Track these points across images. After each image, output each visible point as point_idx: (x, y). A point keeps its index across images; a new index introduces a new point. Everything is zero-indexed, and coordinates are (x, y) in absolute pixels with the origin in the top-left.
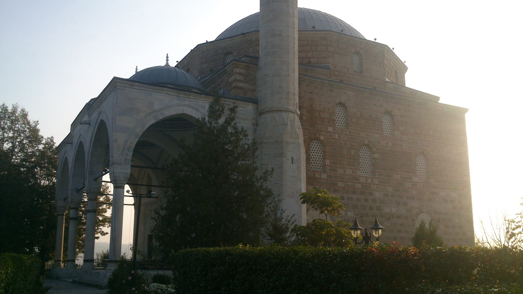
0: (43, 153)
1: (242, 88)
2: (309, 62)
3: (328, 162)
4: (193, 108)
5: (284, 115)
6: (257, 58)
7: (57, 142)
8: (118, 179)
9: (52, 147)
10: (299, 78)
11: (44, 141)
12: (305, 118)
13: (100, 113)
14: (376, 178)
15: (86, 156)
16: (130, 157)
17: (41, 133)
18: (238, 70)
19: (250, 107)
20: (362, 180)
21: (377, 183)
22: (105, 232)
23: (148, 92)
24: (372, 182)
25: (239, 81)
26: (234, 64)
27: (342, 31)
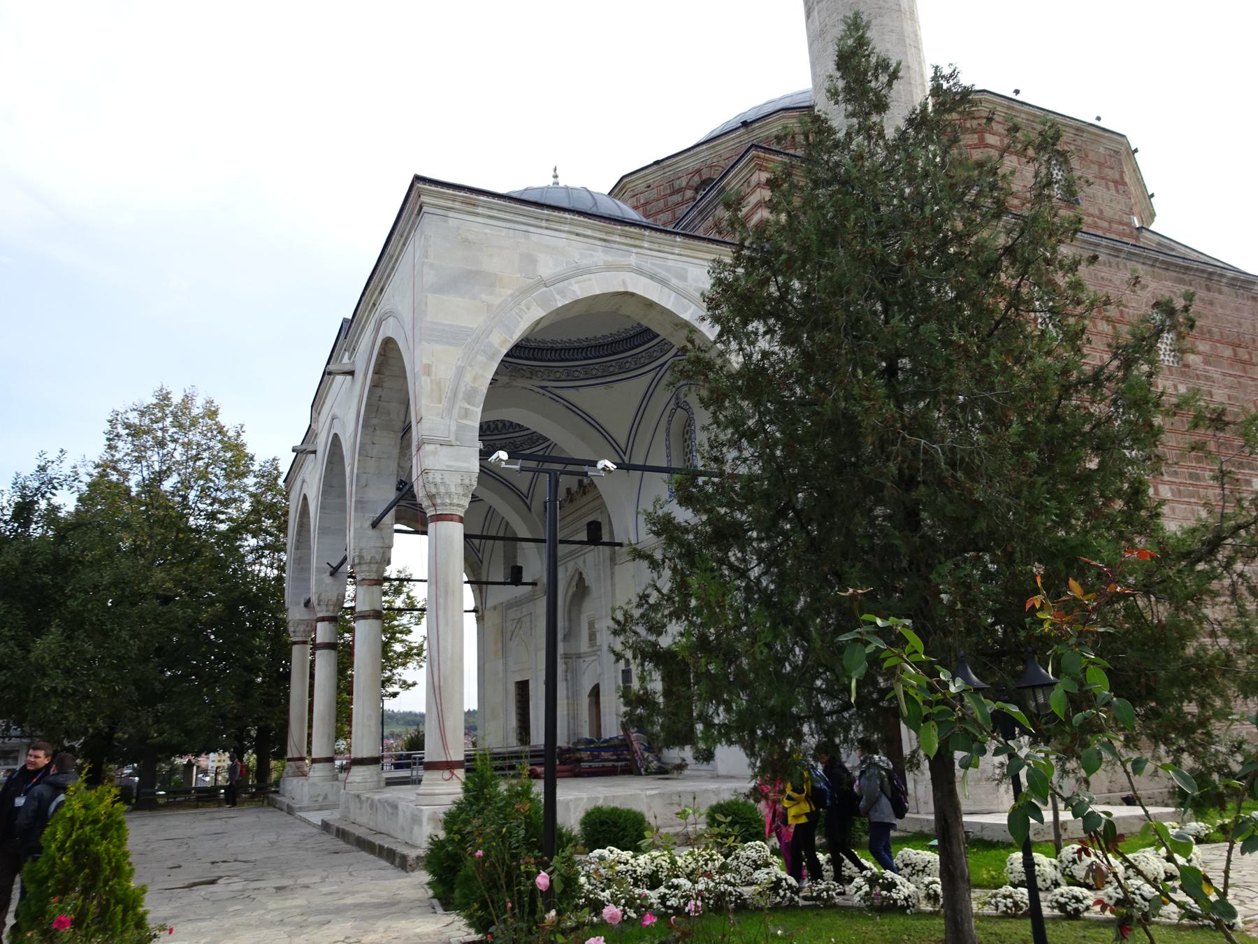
4: (652, 277)
7: (284, 468)
8: (442, 490)
11: (256, 468)
14: (1164, 483)
15: (347, 461)
17: (249, 450)
22: (410, 682)
23: (517, 226)
26: (752, 159)
27: (1017, 92)
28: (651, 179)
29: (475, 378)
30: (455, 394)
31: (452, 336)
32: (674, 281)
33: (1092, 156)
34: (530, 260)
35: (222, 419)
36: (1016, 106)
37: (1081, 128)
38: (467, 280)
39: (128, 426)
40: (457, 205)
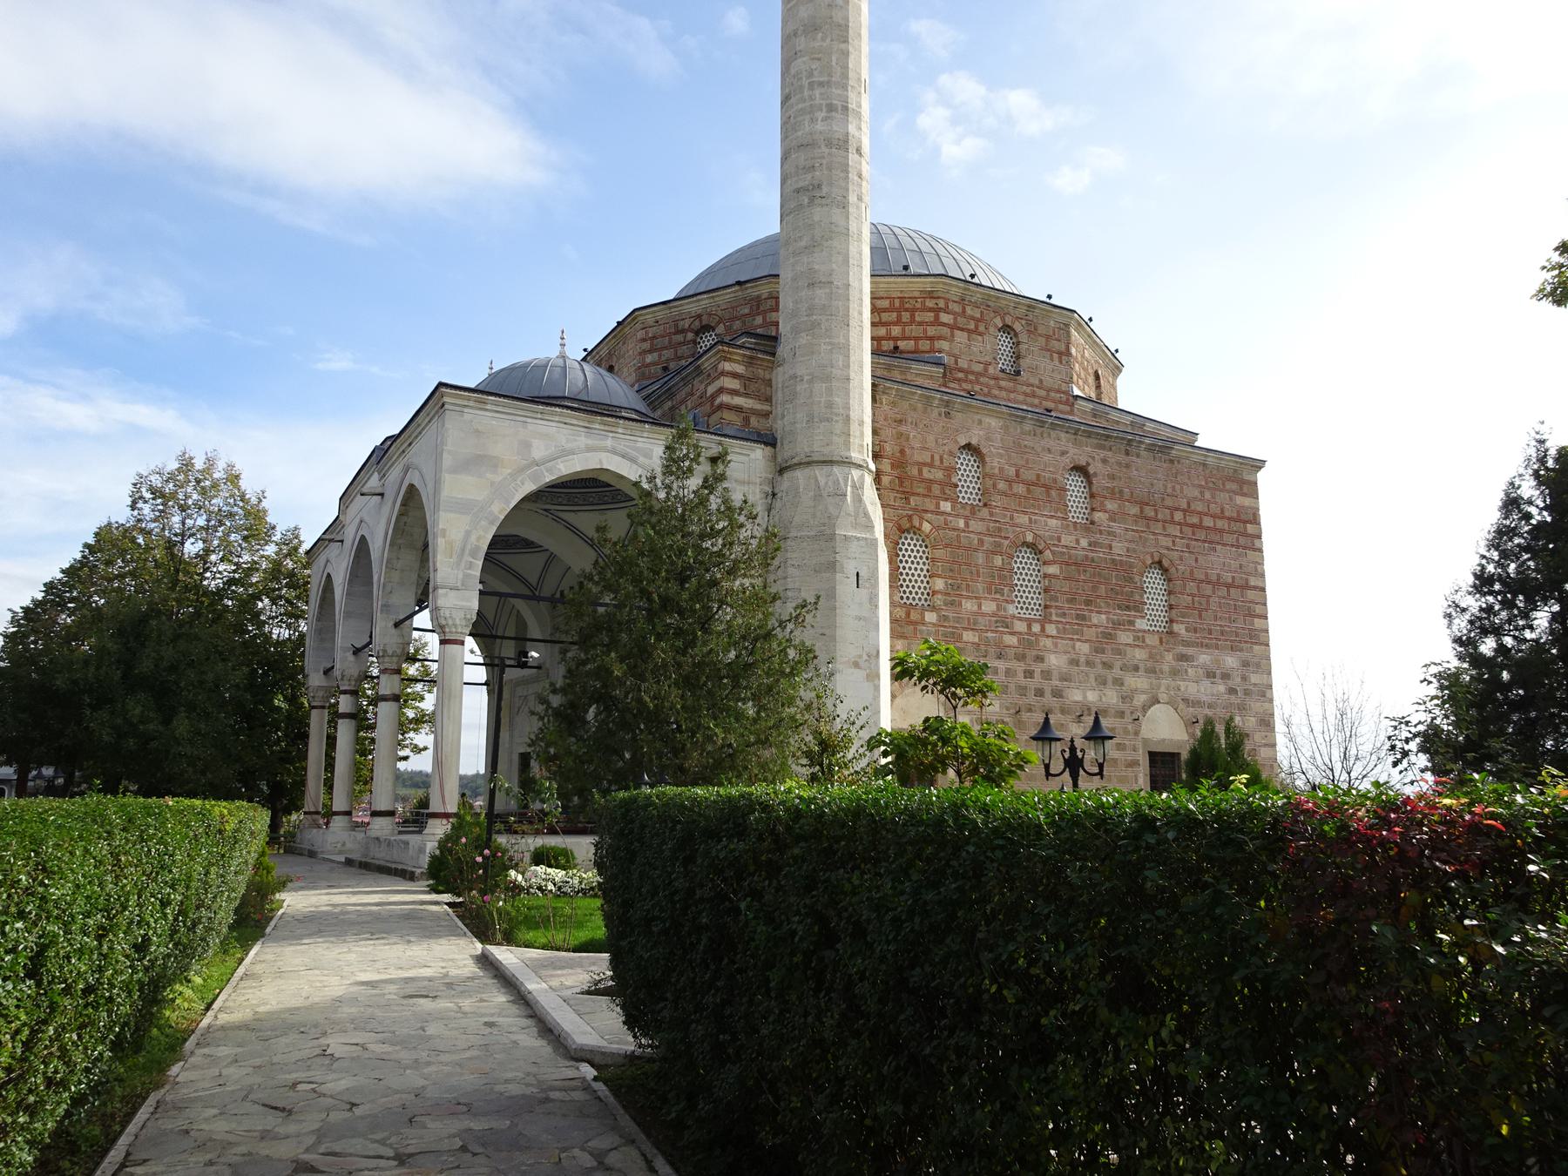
0: (277, 566)
1: (738, 409)
2: (896, 348)
3: (939, 584)
5: (836, 469)
6: (775, 339)
7: (308, 540)
9: (296, 549)
10: (873, 385)
12: (885, 480)
13: (406, 470)
14: (1051, 622)
16: (477, 572)
17: (270, 519)
18: (728, 366)
19: (759, 453)
20: (1020, 627)
21: (1054, 633)
24: (1043, 629)
25: (734, 392)
28: (660, 315)
29: (478, 539)
30: (463, 550)
31: (463, 507)
32: (641, 459)
33: (1041, 330)
34: (526, 445)
35: (243, 484)
36: (973, 288)
37: (1032, 304)
38: (478, 462)
39: (153, 490)
40: (471, 403)
